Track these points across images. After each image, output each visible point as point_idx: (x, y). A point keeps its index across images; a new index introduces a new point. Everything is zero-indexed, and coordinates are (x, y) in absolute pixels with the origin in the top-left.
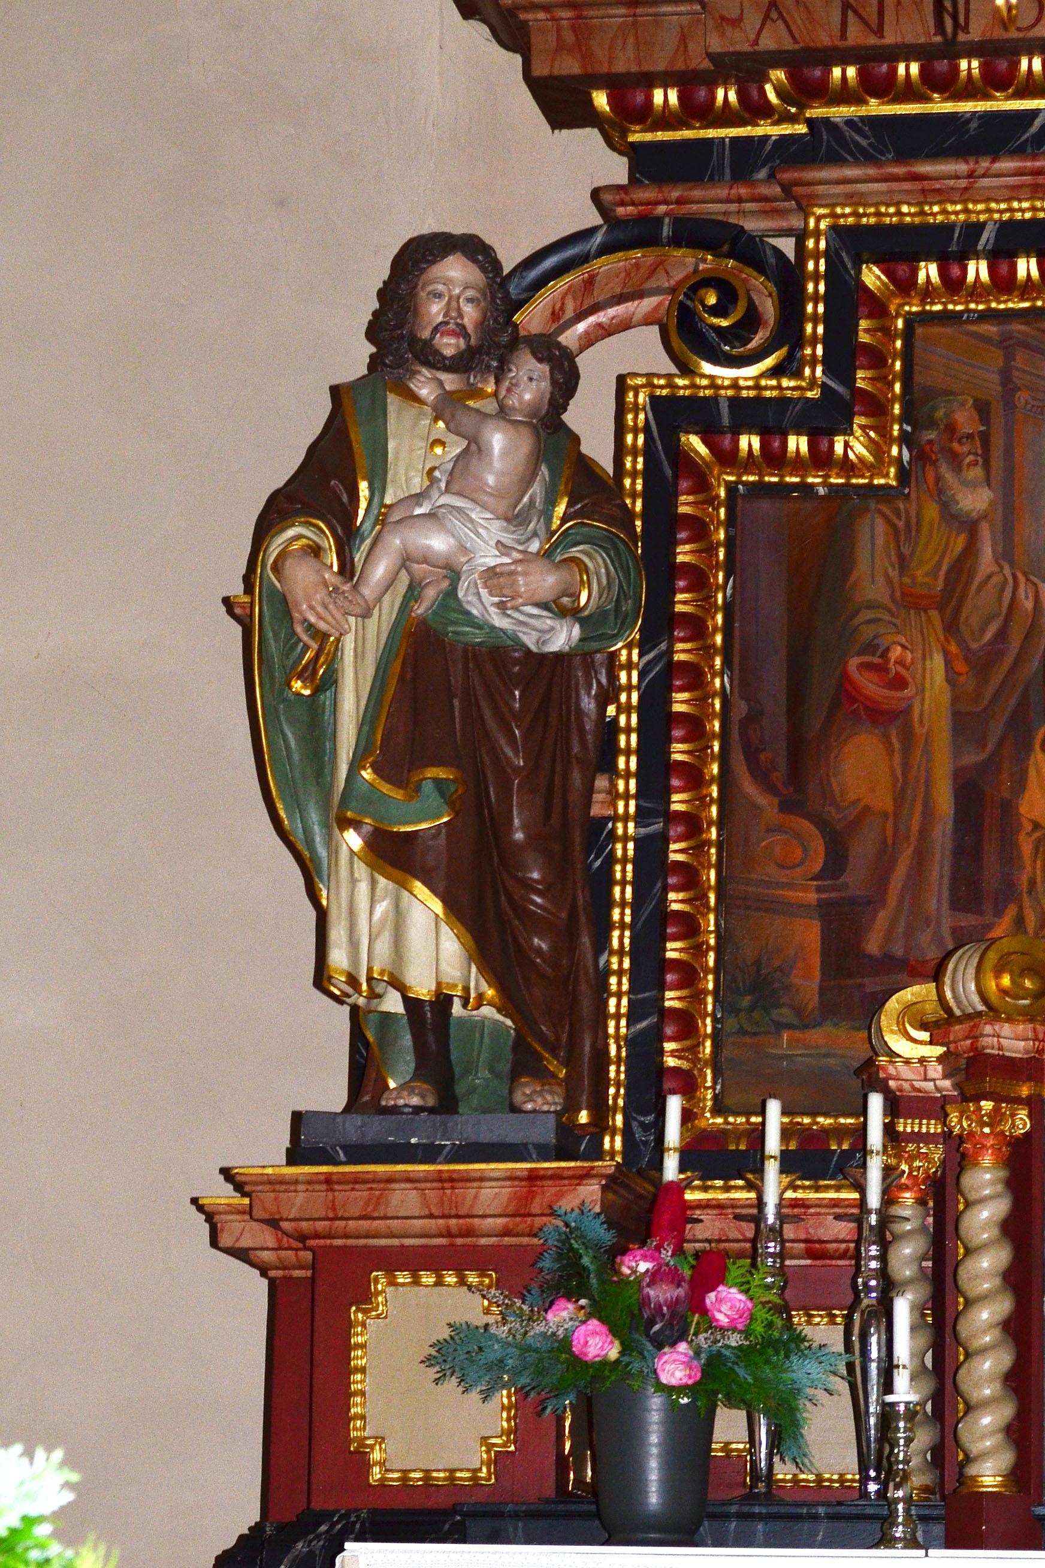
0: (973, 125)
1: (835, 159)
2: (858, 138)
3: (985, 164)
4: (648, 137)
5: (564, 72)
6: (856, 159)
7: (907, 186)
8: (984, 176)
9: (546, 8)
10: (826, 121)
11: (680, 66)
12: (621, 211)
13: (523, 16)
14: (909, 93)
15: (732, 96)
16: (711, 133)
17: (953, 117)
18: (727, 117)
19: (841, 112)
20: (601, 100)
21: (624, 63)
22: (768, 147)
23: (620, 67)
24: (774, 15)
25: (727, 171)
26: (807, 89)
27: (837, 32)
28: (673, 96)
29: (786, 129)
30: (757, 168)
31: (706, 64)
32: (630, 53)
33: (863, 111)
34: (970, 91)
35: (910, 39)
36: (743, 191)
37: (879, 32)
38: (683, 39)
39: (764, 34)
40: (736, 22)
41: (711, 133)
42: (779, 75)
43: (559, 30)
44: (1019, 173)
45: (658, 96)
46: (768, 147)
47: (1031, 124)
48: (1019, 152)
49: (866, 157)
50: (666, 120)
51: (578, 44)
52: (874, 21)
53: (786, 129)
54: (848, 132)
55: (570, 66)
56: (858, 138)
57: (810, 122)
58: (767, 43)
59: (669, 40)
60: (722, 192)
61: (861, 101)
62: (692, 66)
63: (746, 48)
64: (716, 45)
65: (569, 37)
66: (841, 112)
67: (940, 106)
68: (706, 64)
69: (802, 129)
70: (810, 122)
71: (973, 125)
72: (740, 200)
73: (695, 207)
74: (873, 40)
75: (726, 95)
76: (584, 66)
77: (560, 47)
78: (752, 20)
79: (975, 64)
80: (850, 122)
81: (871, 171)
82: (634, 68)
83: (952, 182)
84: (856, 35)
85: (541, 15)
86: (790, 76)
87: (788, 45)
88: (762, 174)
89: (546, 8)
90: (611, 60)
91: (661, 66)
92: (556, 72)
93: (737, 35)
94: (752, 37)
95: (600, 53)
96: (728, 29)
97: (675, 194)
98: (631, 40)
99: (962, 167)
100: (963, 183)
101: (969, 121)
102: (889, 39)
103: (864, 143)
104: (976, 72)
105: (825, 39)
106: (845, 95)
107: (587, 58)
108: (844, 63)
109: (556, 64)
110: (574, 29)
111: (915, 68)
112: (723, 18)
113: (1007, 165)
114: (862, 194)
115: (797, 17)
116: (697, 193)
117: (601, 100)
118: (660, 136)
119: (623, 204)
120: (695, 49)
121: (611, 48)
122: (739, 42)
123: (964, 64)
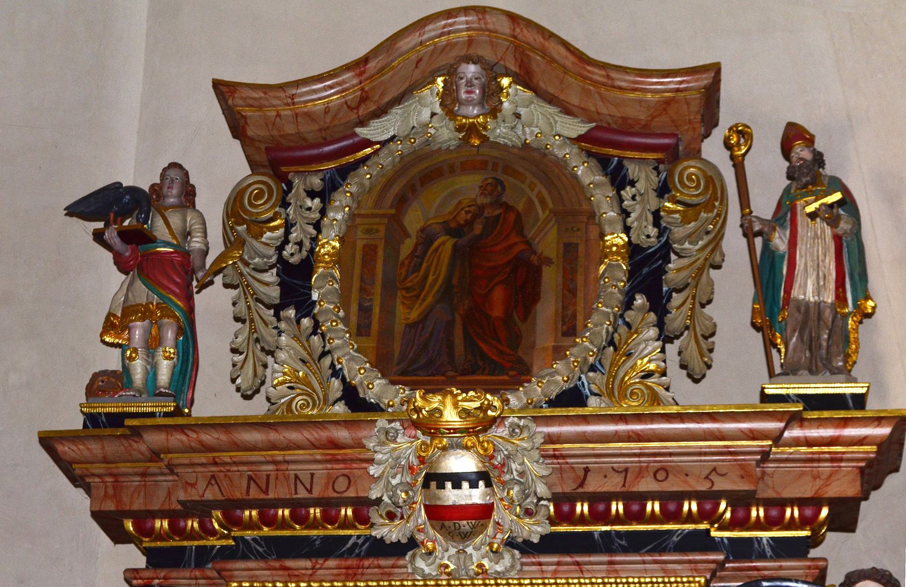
0: (317, 543)
1: (245, 557)
2: (258, 548)
3: (321, 561)
4: (153, 545)
5: (107, 509)
6: (256, 558)
7: (281, 572)
8: (320, 569)
9: (99, 476)
10: (242, 538)
11: (167, 507)
12: (135, 582)
13: (88, 480)
14: (284, 525)
15: (196, 525)
16: (185, 543)
17: (307, 538)
18: (192, 536)
19: (249, 534)
20: (129, 526)
21: (138, 505)
22: (214, 552)
23: (135, 507)
24: (213, 482)
25: (193, 564)
26: (231, 521)
27: (244, 491)
28: (166, 524)
29: (224, 542)
30: (207, 563)
31: (179, 507)
32: (141, 501)
33: (261, 533)
34: (315, 525)
35: (282, 496)
36: (198, 573)
37: (266, 492)
38: (169, 494)
39: (207, 491)
40: (193, 485)
41: (185, 543)
42: (219, 514)
43: (106, 487)
44: (338, 568)
45: (158, 524)
46: (214, 552)
47: (347, 543)
48: (341, 556)
49: (261, 557)
50: (160, 537)
51: (115, 495)
52: (264, 487)
53: (224, 542)
54: (253, 544)
55: (110, 506)
56: (258, 548)
57: (234, 538)
58: (209, 496)
59: (162, 494)
60: (187, 574)
61: (260, 529)
62: (172, 508)
63: (197, 498)
64: (182, 496)
65: (111, 491)
66: (249, 534)
67: (299, 531)
68: (179, 507)
69: (231, 542)
70: (234, 538)
71: (317, 543)
72: (196, 578)
73: (172, 581)
74: (263, 496)
75: (193, 524)
76: (117, 506)
77: (106, 495)
78: (202, 484)
79: (318, 511)
80: (254, 540)
81: (262, 564)
82: (143, 508)
83: (304, 572)
84: (254, 493)
85: (97, 480)
86: (224, 514)
87: (220, 497)
88: (210, 566)
89: (99, 476)
90: (131, 504)
91: (156, 507)
92: (102, 509)
93: (194, 491)
94: (201, 493)
95: (125, 499)
96: (189, 489)
97: (162, 575)
98: (142, 493)
99: (308, 564)
100: (310, 572)
101: (315, 540)
102: (271, 495)
103: (260, 549)
104: (318, 515)
105: (238, 495)
106: (251, 525)
107: (119, 501)
108: (251, 507)
109: (103, 504)
110: (114, 488)
111: (287, 512)
112: (187, 483)
113: (331, 563)
114: (257, 576)
115: (225, 483)
116: (174, 574)
117: (129, 526)
118: (159, 544)
119: (136, 578)
120: (174, 499)
121: (132, 496)
122: (194, 495)
123: (312, 511)
